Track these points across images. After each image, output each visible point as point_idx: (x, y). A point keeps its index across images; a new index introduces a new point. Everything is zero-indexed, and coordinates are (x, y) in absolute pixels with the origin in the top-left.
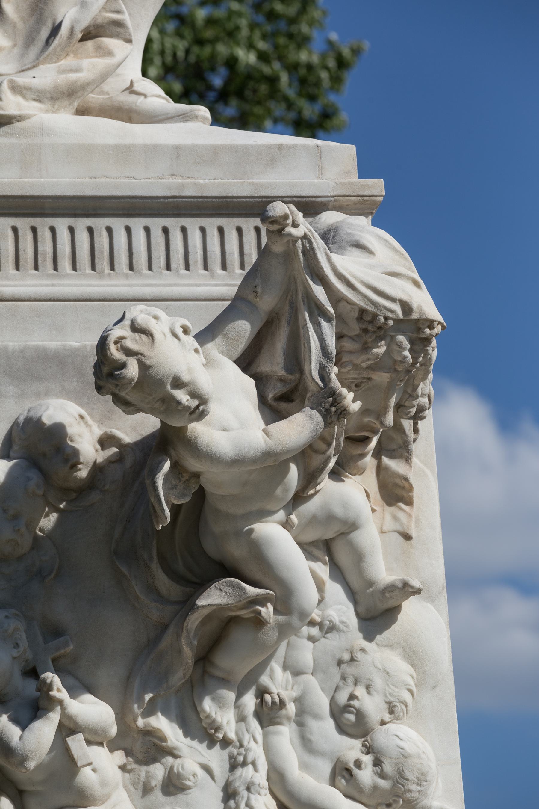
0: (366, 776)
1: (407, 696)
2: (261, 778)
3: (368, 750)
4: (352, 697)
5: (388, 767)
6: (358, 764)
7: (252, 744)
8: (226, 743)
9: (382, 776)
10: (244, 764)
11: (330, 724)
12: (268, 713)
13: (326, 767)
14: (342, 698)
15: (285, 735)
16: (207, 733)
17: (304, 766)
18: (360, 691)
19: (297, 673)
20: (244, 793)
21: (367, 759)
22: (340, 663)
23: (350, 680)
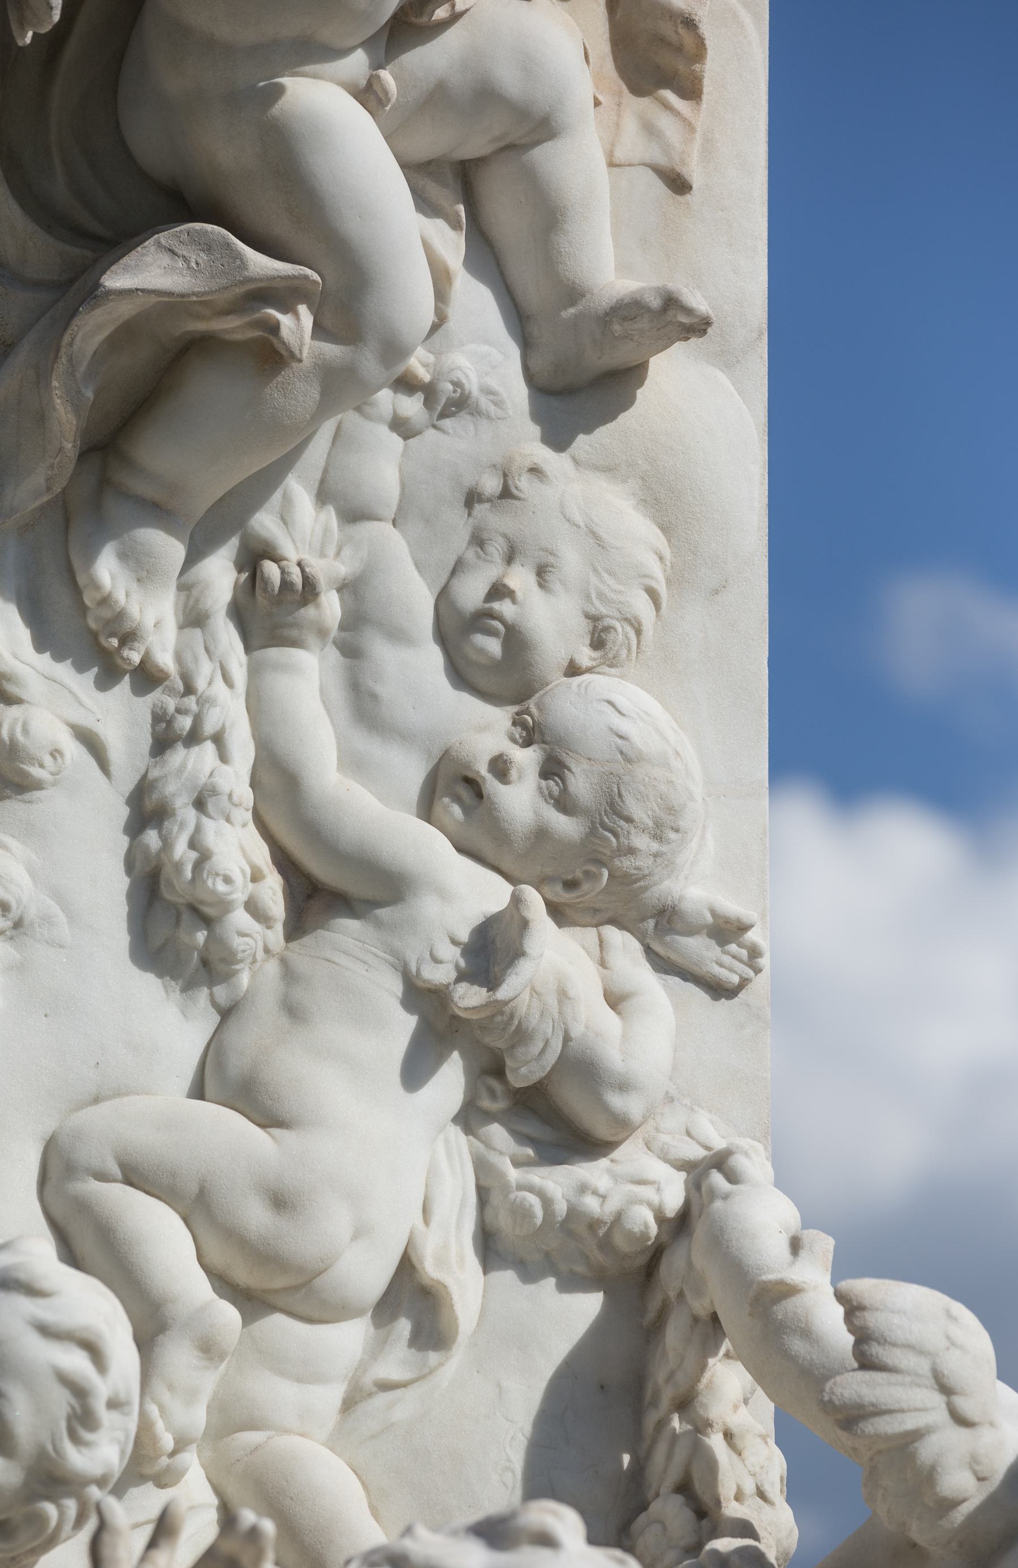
0: (520, 800)
1: (642, 606)
2: (235, 778)
3: (530, 733)
4: (498, 591)
5: (581, 783)
6: (500, 767)
7: (219, 687)
8: (147, 677)
9: (564, 803)
10: (193, 738)
11: (434, 657)
12: (269, 610)
13: (411, 772)
14: (471, 592)
15: (307, 678)
16: (100, 647)
17: (353, 763)
18: (520, 579)
19: (354, 515)
20: (188, 815)
21: (526, 759)
22: (472, 498)
23: (496, 548)
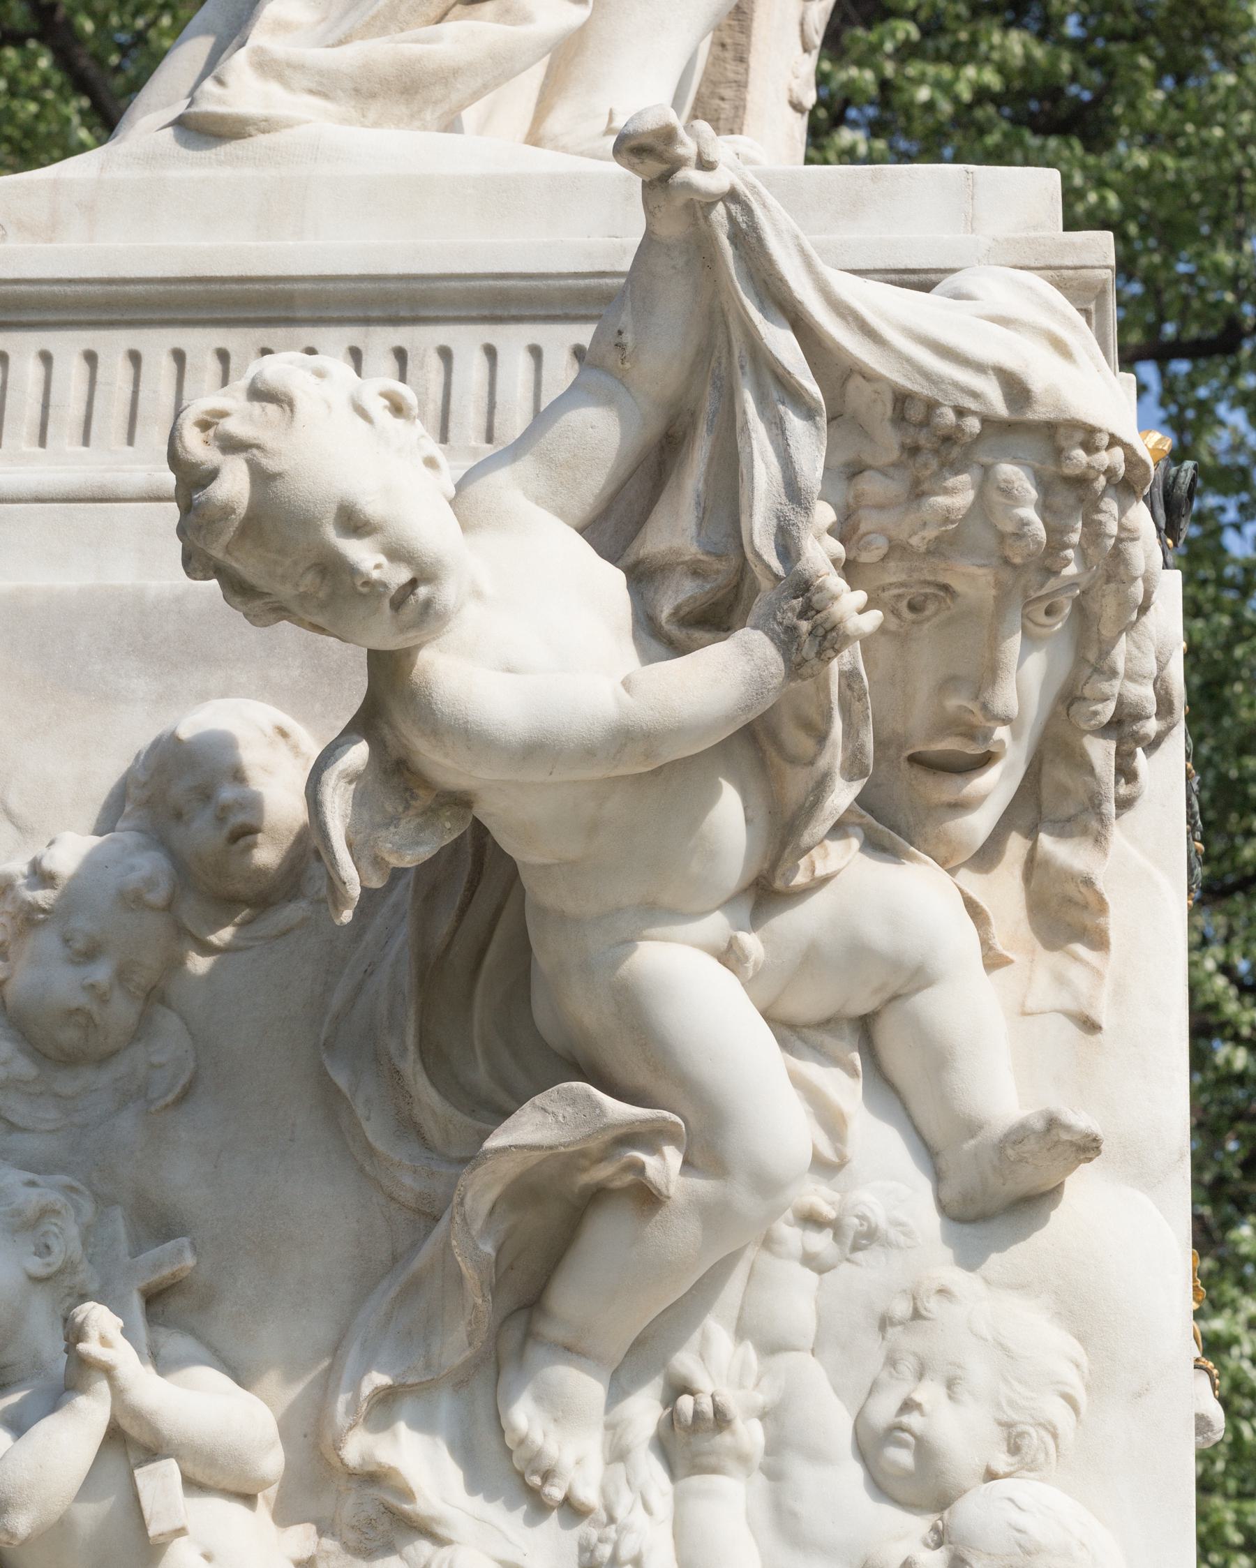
4: (908, 1406)
8: (573, 1510)
11: (855, 1472)
12: (688, 1441)
14: (884, 1411)
16: (525, 1485)
18: (929, 1393)
19: (771, 1348)
22: (885, 1323)
23: (907, 1366)
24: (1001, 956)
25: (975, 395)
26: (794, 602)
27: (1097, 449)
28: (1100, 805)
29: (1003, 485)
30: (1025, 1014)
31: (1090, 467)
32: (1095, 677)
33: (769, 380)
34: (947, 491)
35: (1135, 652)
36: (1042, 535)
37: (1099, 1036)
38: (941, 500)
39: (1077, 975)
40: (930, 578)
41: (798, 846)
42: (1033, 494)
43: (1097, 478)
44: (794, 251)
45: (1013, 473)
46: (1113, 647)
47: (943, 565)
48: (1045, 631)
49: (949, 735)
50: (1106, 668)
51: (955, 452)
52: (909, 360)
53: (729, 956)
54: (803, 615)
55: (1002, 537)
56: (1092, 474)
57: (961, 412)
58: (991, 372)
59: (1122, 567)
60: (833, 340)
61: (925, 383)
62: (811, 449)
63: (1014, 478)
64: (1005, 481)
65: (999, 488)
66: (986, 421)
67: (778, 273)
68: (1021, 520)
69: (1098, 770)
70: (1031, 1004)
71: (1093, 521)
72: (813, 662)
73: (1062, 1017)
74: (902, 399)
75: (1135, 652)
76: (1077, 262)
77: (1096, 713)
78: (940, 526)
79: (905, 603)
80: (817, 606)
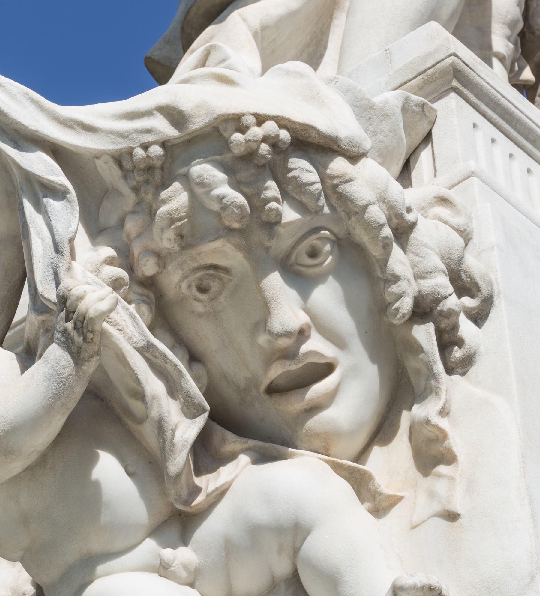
24: (389, 496)
25: (148, 131)
26: (62, 313)
27: (247, 128)
28: (432, 368)
29: (198, 181)
30: (413, 528)
31: (248, 141)
32: (387, 285)
33: (38, 188)
34: (164, 202)
35: (416, 259)
36: (241, 199)
37: (460, 520)
38: (163, 210)
39: (440, 487)
40: (196, 265)
41: (169, 476)
42: (221, 176)
43: (259, 147)
44: (28, 104)
45: (204, 170)
46: (387, 261)
47: (194, 252)
48: (316, 270)
49: (272, 363)
50: (389, 277)
51: (158, 175)
52: (112, 132)
53: (163, 569)
54: (67, 320)
55: (218, 215)
56: (254, 146)
57: (145, 147)
58: (156, 112)
59: (349, 203)
60: (76, 146)
61: (121, 140)
62: (66, 215)
63: (202, 172)
64: (198, 177)
65: (198, 184)
66: (163, 144)
67: (13, 119)
68: (218, 196)
69: (425, 347)
70: (416, 520)
71: (290, 178)
72: (84, 347)
73: (436, 518)
74: (120, 159)
75: (416, 259)
76: (433, 62)
77: (397, 309)
78: (170, 226)
79: (194, 290)
80: (72, 310)
